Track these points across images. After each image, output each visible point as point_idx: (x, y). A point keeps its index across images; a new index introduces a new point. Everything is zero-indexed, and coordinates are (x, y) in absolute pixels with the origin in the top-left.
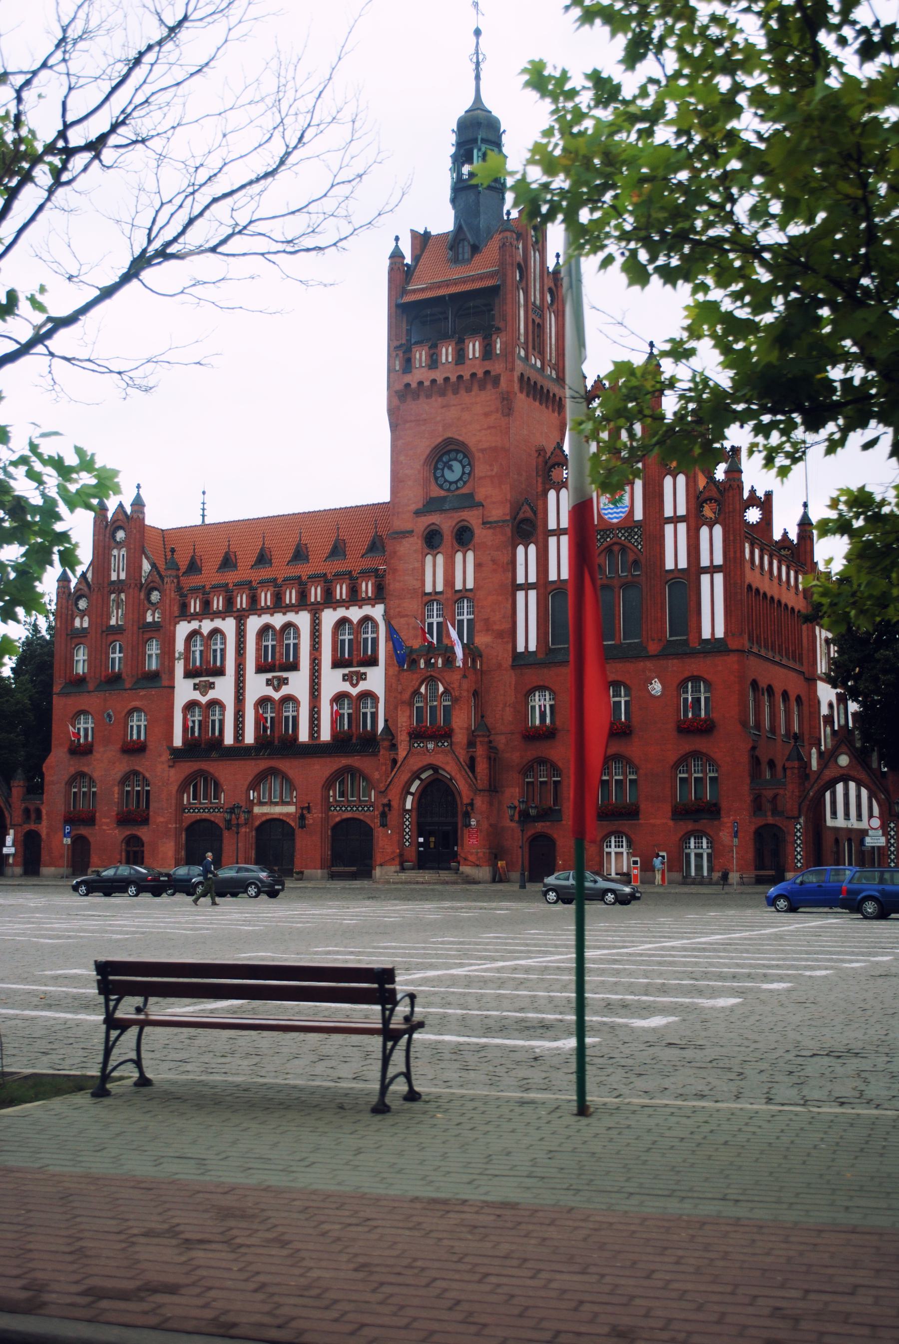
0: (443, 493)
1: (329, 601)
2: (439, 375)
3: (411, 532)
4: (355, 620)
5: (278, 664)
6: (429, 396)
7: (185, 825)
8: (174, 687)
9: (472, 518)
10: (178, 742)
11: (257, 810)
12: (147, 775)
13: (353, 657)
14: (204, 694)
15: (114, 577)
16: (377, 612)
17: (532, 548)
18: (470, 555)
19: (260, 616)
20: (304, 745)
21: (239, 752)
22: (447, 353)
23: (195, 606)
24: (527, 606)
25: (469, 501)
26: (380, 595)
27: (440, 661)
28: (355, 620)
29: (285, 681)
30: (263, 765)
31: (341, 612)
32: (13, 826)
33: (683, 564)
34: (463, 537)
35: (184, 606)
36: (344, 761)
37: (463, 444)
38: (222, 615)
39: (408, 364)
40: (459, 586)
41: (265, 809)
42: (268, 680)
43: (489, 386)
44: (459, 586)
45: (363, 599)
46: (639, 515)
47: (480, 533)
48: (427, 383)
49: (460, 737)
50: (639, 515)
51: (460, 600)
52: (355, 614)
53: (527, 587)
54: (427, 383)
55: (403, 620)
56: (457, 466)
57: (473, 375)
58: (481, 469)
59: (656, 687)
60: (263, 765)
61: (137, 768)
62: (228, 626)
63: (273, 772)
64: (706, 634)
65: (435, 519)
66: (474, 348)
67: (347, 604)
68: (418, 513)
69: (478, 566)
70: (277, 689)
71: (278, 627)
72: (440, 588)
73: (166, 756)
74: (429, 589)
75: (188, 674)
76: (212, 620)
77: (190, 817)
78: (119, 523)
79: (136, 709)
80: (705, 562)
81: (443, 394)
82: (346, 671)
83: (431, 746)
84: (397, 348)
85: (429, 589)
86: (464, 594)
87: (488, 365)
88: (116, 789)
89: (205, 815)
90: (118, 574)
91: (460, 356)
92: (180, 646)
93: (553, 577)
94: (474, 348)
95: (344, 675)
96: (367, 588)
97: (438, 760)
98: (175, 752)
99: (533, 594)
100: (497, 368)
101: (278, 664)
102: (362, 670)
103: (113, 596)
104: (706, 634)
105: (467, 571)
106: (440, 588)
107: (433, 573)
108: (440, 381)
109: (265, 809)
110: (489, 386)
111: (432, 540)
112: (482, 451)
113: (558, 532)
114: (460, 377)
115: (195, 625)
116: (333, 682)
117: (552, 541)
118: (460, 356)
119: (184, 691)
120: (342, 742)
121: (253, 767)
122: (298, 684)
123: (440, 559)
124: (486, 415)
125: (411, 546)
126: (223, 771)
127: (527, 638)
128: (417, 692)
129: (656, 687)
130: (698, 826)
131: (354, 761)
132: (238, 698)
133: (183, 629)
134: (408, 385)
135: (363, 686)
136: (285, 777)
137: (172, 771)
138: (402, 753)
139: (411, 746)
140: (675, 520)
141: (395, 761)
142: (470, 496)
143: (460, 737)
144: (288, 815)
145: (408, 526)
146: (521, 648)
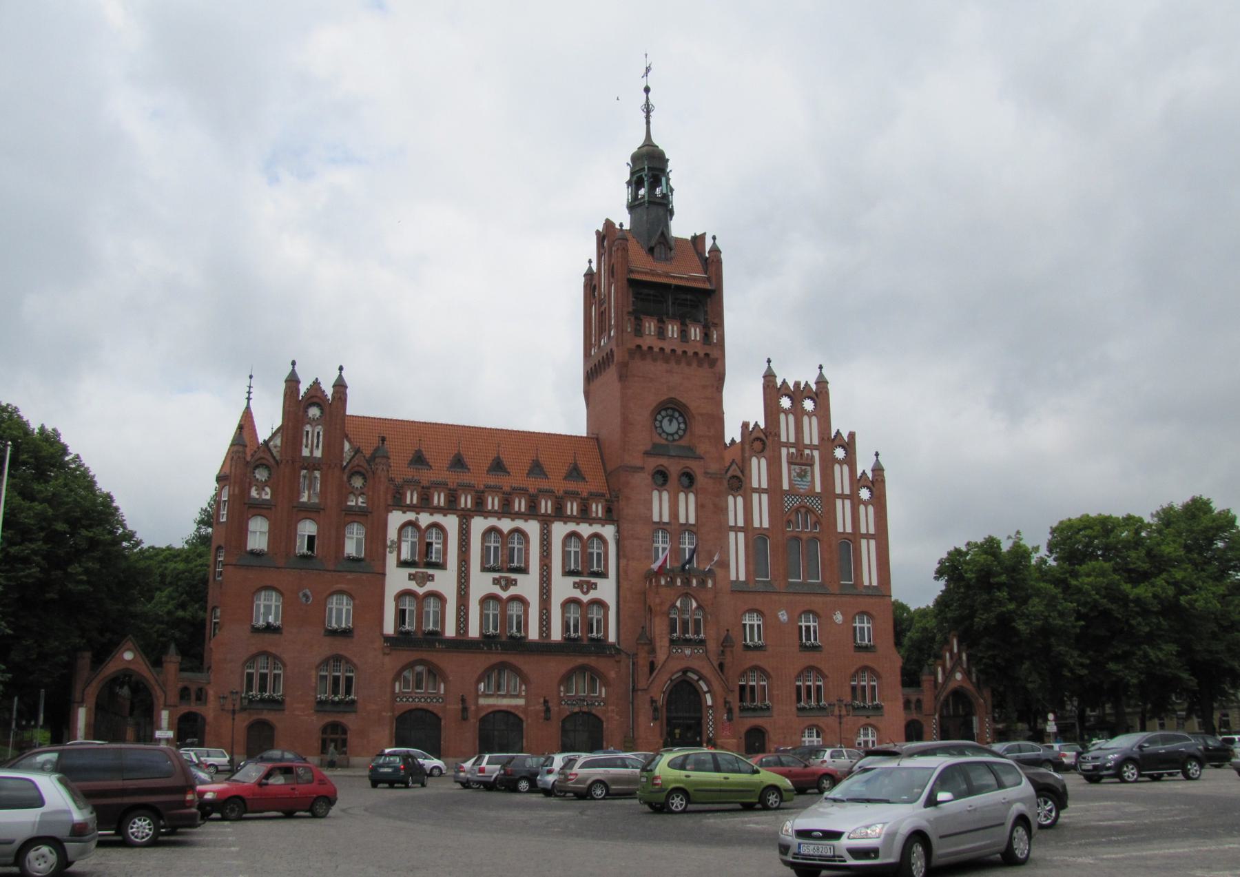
0: (664, 442)
1: (559, 514)
2: (668, 347)
3: (642, 468)
4: (585, 536)
5: (506, 563)
6: (655, 360)
7: (397, 713)
8: (384, 575)
9: (695, 467)
10: (389, 628)
11: (482, 701)
12: (355, 661)
13: (585, 568)
14: (421, 584)
15: (306, 452)
16: (608, 531)
17: (740, 500)
18: (692, 497)
19: (486, 518)
20: (534, 643)
21: (461, 644)
22: (673, 330)
23: (411, 497)
24: (737, 545)
25: (690, 452)
26: (610, 516)
27: (694, 581)
28: (585, 536)
29: (514, 582)
30: (495, 659)
31: (571, 527)
32: (166, 706)
33: (849, 529)
34: (688, 481)
35: (404, 496)
36: (581, 661)
37: (684, 405)
38: (444, 511)
39: (638, 332)
40: (682, 520)
41: (491, 701)
42: (494, 579)
43: (706, 365)
44: (682, 520)
45: (568, 517)
46: (818, 489)
47: (701, 480)
48: (656, 350)
49: (712, 646)
50: (818, 489)
51: (657, 531)
52: (585, 530)
53: (736, 529)
54: (656, 350)
55: (636, 542)
56: (675, 423)
57: (696, 354)
58: (699, 428)
59: (839, 617)
60: (495, 659)
61: (342, 653)
62: (451, 523)
63: (502, 667)
64: (866, 583)
65: (663, 461)
66: (695, 333)
67: (578, 520)
68: (647, 453)
69: (699, 507)
70: (505, 588)
71: (506, 531)
72: (666, 519)
73: (380, 643)
74: (656, 518)
75: (403, 564)
76: (431, 514)
77: (405, 704)
78: (315, 400)
79: (341, 592)
80: (863, 531)
81: (667, 361)
82: (577, 579)
83: (688, 652)
84: (629, 313)
85: (656, 518)
86: (687, 528)
87: (708, 350)
88: (313, 672)
89: (422, 705)
90: (313, 449)
91: (684, 334)
92: (392, 534)
93: (756, 524)
94: (695, 333)
95: (575, 583)
96: (597, 509)
97: (696, 664)
98: (387, 639)
99: (741, 536)
100: (714, 354)
101: (506, 563)
102: (593, 580)
103: (304, 472)
104: (866, 583)
105: (688, 508)
106: (666, 519)
107: (660, 507)
108: (668, 351)
109: (491, 701)
110: (706, 365)
111: (661, 478)
112: (702, 415)
113: (760, 491)
114: (685, 352)
115: (411, 516)
116: (563, 588)
117: (755, 496)
118: (684, 334)
119: (397, 580)
120: (570, 646)
121: (482, 661)
122: (528, 586)
123: (665, 495)
124: (705, 387)
125: (642, 480)
126: (449, 662)
127: (738, 570)
128: (673, 606)
129: (839, 617)
130: (868, 721)
131: (591, 661)
132: (461, 593)
133: (396, 519)
134: (639, 347)
135: (593, 595)
136: (517, 671)
137: (387, 659)
138: (661, 656)
139: (670, 651)
140: (843, 497)
141: (652, 667)
142: (690, 449)
143: (712, 646)
144: (517, 707)
145: (639, 463)
146: (733, 577)
